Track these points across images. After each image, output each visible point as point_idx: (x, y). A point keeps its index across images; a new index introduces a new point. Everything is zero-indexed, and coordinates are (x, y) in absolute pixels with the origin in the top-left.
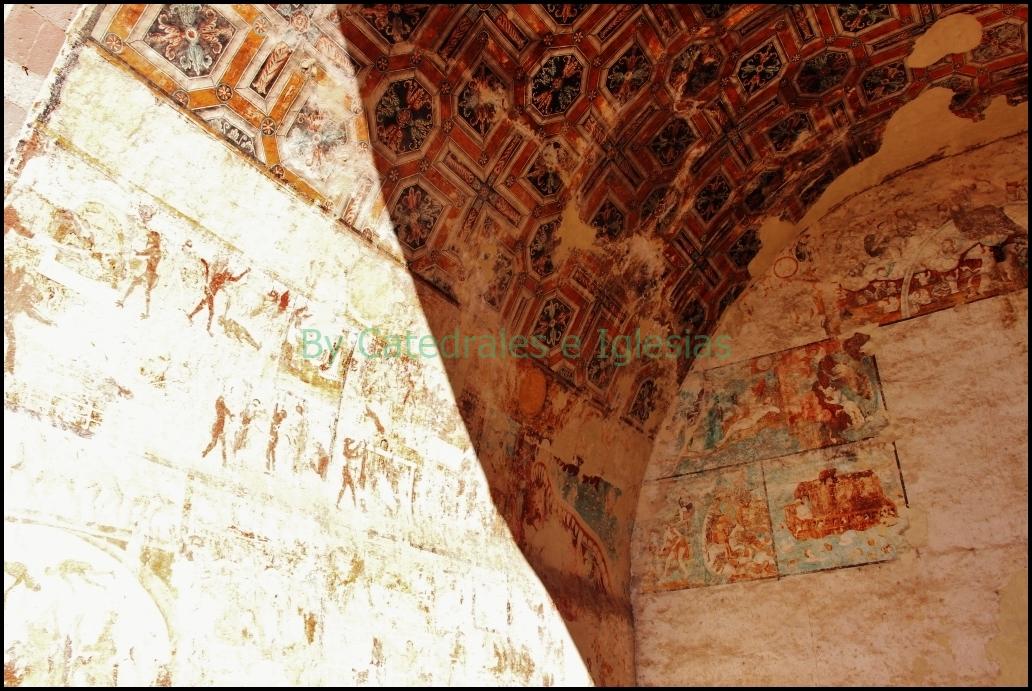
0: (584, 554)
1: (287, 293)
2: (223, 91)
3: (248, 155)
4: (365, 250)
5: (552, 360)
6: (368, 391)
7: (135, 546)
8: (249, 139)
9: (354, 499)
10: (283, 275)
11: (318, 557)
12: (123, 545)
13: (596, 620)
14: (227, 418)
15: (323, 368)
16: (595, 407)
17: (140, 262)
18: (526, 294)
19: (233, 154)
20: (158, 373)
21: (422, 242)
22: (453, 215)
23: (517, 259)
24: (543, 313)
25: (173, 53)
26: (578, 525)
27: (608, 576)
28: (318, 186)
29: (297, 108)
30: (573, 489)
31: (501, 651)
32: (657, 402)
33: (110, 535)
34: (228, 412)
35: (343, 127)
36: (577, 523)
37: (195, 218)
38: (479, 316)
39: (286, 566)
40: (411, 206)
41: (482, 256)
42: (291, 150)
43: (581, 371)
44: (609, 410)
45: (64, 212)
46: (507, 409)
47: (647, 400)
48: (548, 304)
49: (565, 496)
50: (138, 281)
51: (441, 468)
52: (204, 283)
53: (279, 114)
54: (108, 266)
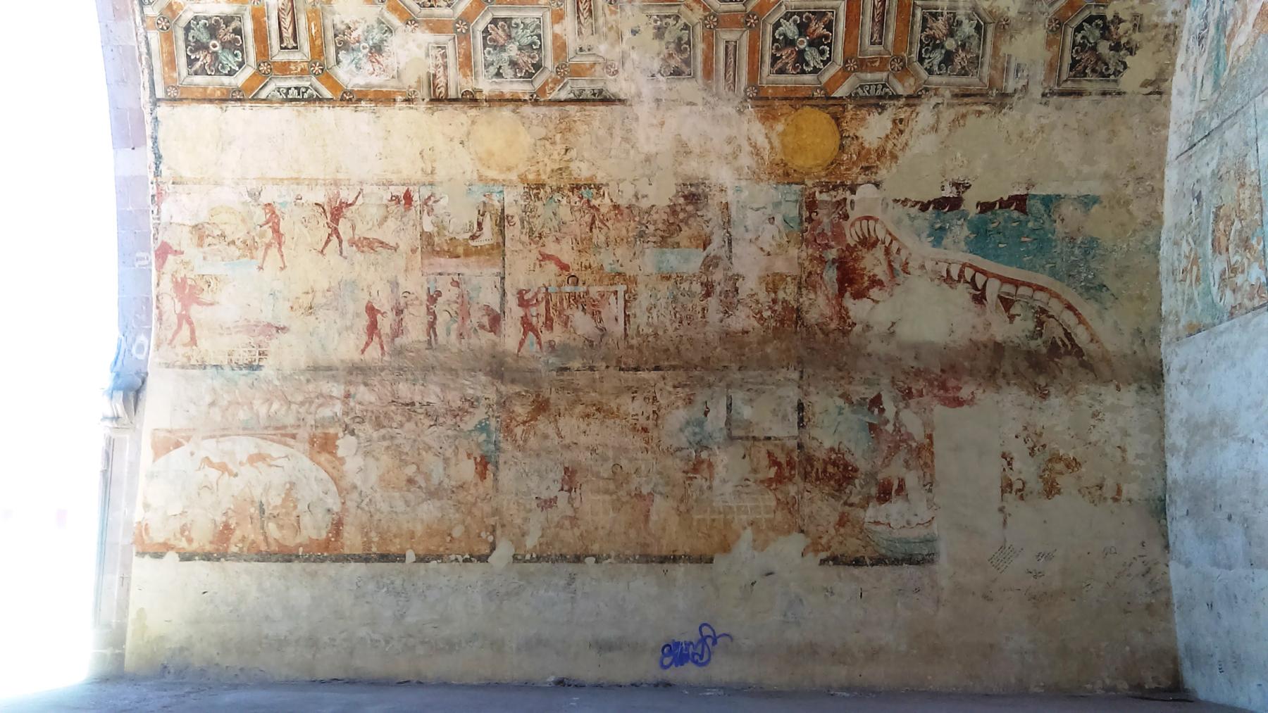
0: (1007, 309)
1: (407, 191)
2: (263, 68)
3: (315, 101)
4: (473, 112)
5: (827, 89)
6: (536, 237)
7: (303, 434)
8: (307, 89)
9: (540, 343)
10: (394, 178)
11: (490, 406)
12: (294, 437)
13: (1030, 400)
14: (379, 317)
15: (473, 237)
16: (966, 104)
17: (265, 231)
18: (726, 35)
19: (300, 109)
20: (306, 304)
21: (538, 66)
22: (558, 17)
23: (688, 6)
24: (775, 40)
25: (212, 68)
26: (984, 272)
27: (1088, 328)
28: (391, 85)
29: (330, 34)
30: (956, 229)
31: (782, 459)
32: (1137, 37)
33: (283, 432)
34: (378, 311)
35: (380, 22)
36: (977, 270)
37: (295, 175)
38: (663, 97)
39: (450, 421)
40: (501, 41)
41: (627, 35)
42: (347, 72)
43: (904, 70)
44: (1004, 95)
45: (197, 226)
46: (765, 177)
47: (1104, 48)
48: (777, 25)
49: (937, 242)
50: (269, 246)
51: (668, 278)
52: (323, 221)
53: (318, 51)
54: (242, 246)
